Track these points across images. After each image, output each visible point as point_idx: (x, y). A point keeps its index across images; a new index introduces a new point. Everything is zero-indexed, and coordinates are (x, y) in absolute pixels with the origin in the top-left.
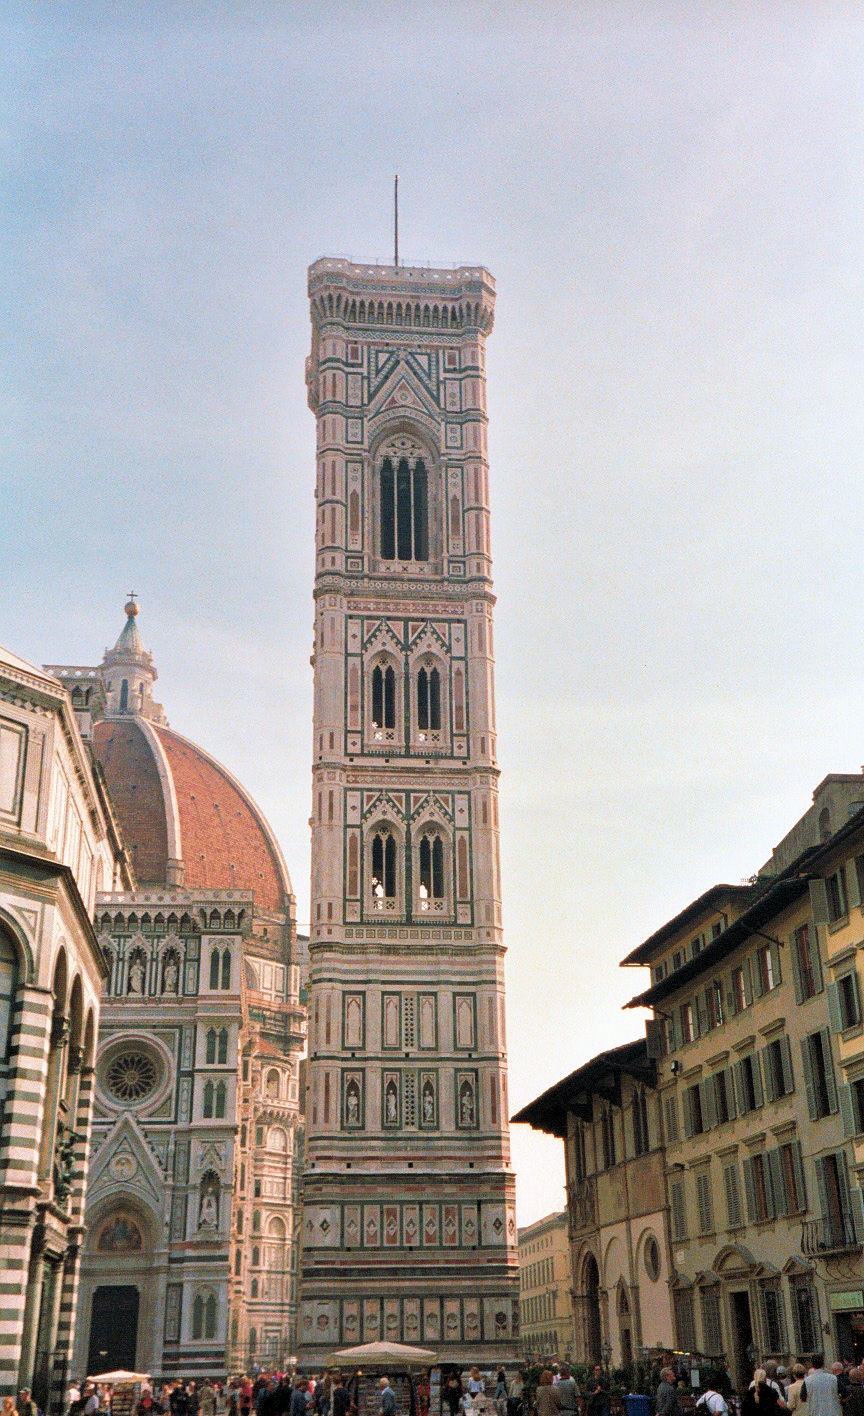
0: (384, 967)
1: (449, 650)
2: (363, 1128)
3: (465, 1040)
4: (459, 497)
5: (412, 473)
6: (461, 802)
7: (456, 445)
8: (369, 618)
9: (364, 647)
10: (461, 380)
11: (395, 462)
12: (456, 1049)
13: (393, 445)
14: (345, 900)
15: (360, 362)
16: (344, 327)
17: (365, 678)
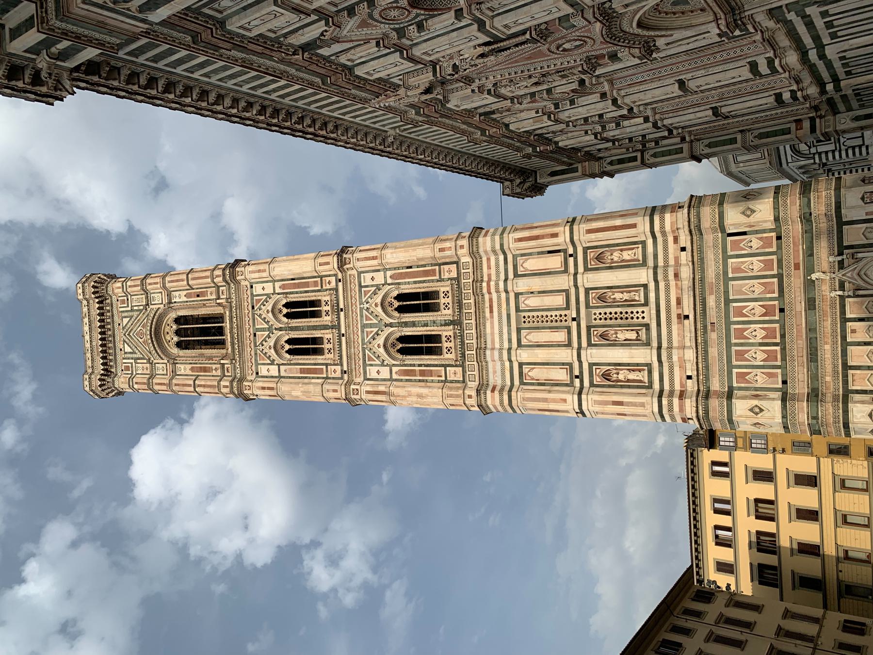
0: (497, 346)
1: (268, 296)
2: (649, 366)
3: (555, 262)
4: (185, 293)
5: (181, 327)
6: (367, 279)
7: (160, 296)
8: (256, 360)
9: (272, 363)
10: (131, 296)
11: (176, 339)
12: (566, 271)
13: (169, 341)
14: (446, 381)
15: (130, 365)
16: (117, 375)
17: (292, 362)
